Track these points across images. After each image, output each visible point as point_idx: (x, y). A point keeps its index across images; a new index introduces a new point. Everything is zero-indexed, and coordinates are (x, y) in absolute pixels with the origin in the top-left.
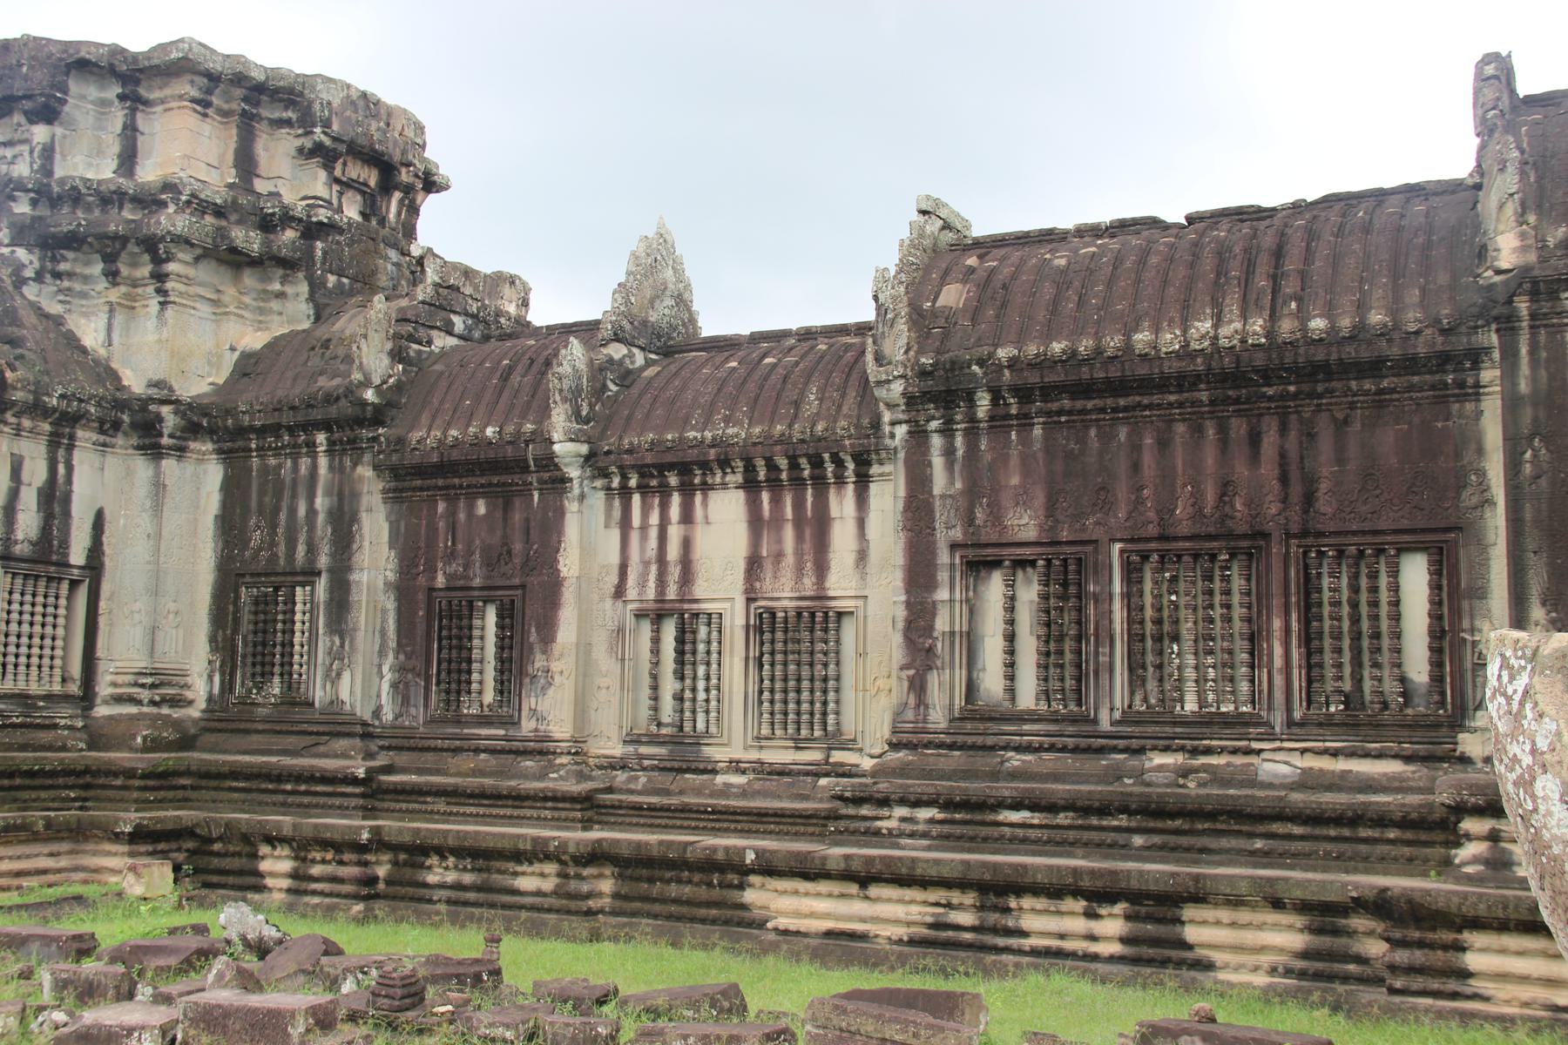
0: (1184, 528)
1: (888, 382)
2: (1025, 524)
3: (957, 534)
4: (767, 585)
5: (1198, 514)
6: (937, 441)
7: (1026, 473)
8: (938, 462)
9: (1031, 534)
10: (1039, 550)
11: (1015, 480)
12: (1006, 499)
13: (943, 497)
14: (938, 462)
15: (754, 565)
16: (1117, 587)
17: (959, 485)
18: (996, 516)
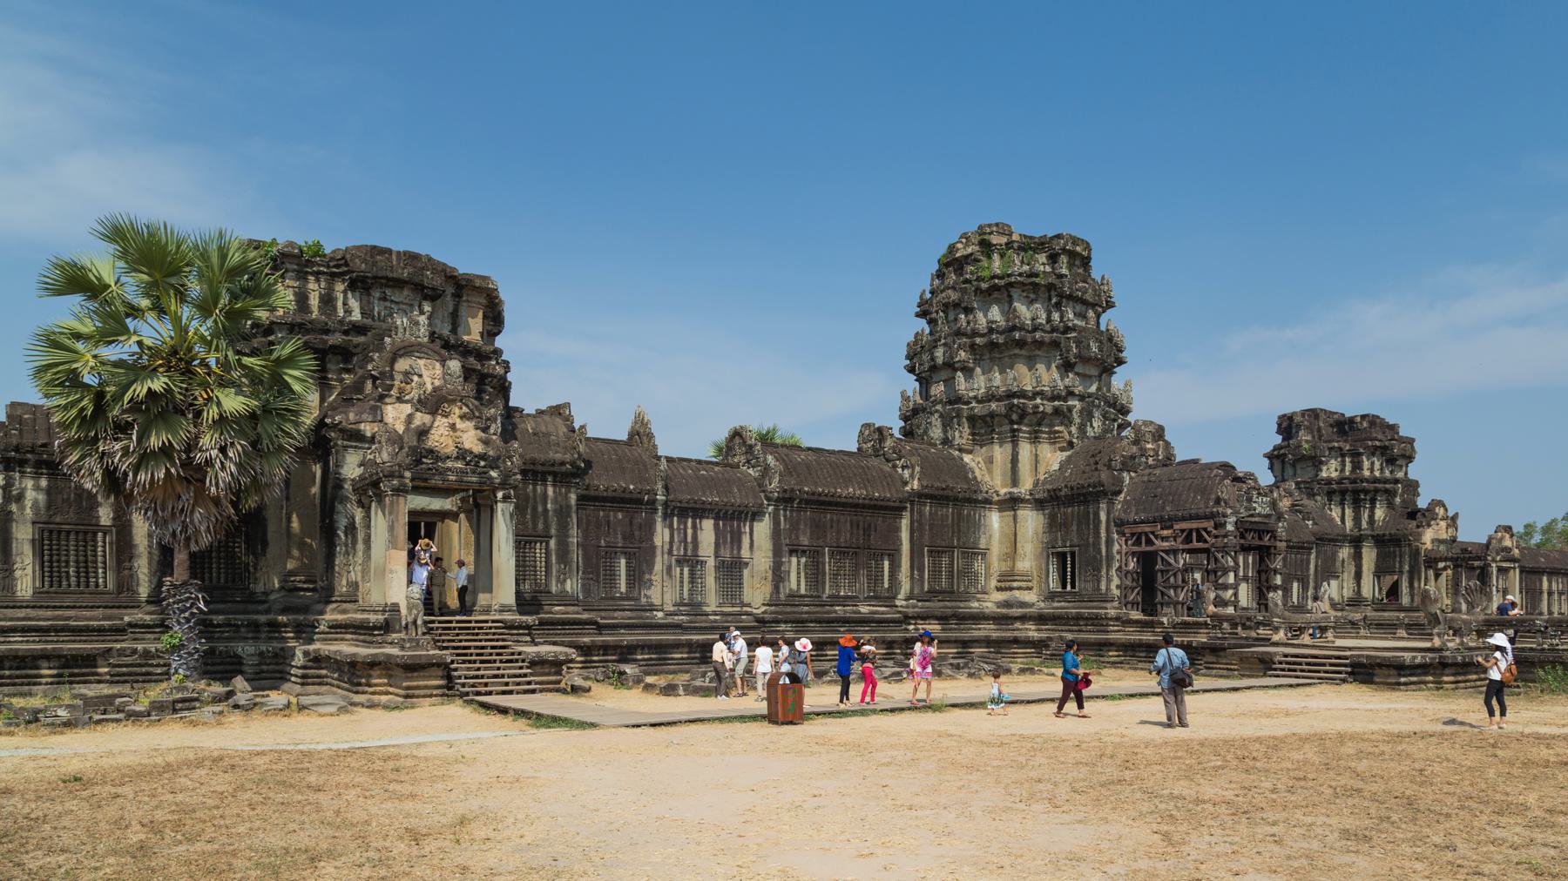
2: (805, 540)
4: (722, 552)
15: (717, 545)
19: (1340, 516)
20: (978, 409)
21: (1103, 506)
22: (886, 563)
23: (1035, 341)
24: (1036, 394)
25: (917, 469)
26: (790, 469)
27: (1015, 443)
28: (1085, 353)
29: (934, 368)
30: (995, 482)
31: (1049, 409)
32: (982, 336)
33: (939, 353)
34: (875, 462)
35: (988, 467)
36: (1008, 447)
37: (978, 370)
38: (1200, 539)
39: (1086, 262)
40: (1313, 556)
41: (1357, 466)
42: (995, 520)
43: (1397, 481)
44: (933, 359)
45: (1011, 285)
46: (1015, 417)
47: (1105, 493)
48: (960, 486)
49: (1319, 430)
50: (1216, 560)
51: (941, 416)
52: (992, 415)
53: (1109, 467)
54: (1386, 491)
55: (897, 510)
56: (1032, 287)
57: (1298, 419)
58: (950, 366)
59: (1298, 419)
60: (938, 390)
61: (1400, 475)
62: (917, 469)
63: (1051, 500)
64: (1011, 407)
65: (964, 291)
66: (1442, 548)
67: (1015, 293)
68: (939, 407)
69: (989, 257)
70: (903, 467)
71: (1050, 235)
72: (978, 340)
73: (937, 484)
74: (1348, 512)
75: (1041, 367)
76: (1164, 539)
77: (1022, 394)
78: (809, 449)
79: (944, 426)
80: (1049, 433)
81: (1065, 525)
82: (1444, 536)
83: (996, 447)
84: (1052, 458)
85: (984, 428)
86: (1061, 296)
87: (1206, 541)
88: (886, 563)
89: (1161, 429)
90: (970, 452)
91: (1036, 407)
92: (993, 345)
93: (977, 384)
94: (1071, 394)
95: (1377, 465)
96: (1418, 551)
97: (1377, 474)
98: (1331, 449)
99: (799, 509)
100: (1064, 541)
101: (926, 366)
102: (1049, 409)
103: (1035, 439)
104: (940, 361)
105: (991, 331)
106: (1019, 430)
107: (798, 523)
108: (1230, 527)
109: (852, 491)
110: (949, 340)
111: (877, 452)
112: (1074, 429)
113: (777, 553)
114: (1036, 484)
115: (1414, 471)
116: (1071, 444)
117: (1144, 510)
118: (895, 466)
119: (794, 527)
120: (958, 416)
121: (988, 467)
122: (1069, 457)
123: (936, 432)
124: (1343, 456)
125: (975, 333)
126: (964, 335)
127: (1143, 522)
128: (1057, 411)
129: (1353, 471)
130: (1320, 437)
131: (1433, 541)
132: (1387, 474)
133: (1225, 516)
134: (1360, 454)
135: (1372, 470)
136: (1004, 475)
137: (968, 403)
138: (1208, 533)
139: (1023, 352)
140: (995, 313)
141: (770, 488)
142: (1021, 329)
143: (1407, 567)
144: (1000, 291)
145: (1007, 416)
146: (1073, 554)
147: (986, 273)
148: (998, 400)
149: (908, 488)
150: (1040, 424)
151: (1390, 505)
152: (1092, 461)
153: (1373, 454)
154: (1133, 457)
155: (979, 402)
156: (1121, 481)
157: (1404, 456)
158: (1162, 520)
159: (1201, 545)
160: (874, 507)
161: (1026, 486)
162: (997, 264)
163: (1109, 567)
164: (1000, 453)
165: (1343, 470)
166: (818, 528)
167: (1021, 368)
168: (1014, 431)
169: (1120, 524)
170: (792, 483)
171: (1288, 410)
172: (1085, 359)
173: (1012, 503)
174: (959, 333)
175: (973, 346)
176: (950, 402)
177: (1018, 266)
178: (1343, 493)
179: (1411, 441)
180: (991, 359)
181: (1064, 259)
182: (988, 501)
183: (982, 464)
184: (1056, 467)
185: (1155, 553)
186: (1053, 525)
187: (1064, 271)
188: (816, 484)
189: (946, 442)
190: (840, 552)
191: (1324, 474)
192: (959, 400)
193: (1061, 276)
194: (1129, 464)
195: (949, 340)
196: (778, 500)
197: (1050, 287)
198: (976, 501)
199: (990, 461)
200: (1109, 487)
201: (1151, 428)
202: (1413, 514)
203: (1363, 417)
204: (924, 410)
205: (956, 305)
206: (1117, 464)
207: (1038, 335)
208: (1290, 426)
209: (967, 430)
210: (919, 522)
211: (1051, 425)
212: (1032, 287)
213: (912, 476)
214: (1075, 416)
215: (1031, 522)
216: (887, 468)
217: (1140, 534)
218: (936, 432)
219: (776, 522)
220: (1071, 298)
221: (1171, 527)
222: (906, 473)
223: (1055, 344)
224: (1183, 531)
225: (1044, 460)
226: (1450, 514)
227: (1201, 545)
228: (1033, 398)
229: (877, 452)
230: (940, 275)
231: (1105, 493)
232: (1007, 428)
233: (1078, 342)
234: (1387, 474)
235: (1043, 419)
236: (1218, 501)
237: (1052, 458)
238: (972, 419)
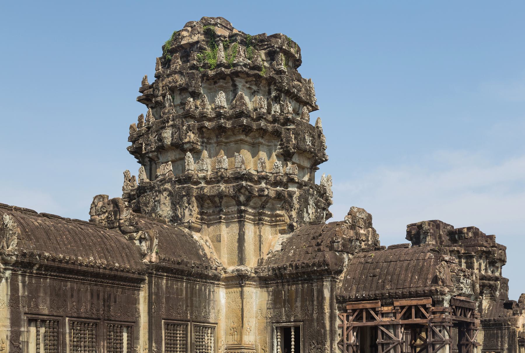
0: (83, 315)
1: (12, 255)
2: (44, 309)
3: (26, 310)
5: (86, 312)
6: (20, 278)
7: (46, 293)
8: (20, 284)
9: (46, 312)
10: (48, 317)
11: (41, 294)
12: (40, 300)
13: (22, 296)
14: (20, 284)
16: (68, 331)
17: (26, 293)
18: (37, 306)
20: (208, 190)
21: (327, 284)
22: (125, 335)
23: (260, 129)
24: (262, 178)
25: (156, 241)
26: (28, 233)
27: (241, 223)
28: (301, 145)
29: (161, 149)
30: (223, 260)
31: (272, 194)
32: (210, 120)
33: (168, 135)
34: (111, 233)
35: (217, 245)
36: (235, 227)
37: (205, 153)
38: (419, 314)
39: (297, 63)
42: (222, 297)
43: (497, 279)
44: (161, 139)
45: (236, 74)
46: (242, 198)
47: (328, 272)
48: (194, 262)
49: (440, 237)
50: (434, 333)
51: (170, 194)
52: (221, 195)
53: (331, 248)
54: (490, 286)
55: (135, 282)
56: (255, 79)
57: (426, 227)
58: (179, 147)
59: (426, 227)
60: (165, 169)
61: (497, 274)
62: (156, 241)
63: (276, 279)
64: (239, 189)
65: (191, 77)
67: (240, 83)
68: (168, 186)
69: (213, 47)
70: (141, 240)
71: (268, 34)
72: (207, 124)
73: (173, 258)
75: (263, 155)
76: (383, 315)
77: (248, 177)
78: (44, 215)
79: (174, 205)
80: (271, 216)
81: (289, 302)
83: (223, 227)
84: (274, 241)
85: (212, 208)
86: (280, 90)
87: (424, 317)
88: (125, 335)
89: (370, 217)
90: (199, 230)
91: (262, 190)
92: (221, 130)
93: (202, 166)
94: (291, 181)
95: (483, 267)
96: (514, 332)
97: (483, 272)
99: (39, 276)
100: (288, 316)
101: (154, 146)
102: (272, 194)
103: (258, 221)
104: (168, 141)
105: (219, 115)
106: (245, 211)
107: (37, 290)
108: (446, 305)
109: (92, 259)
110: (178, 122)
111: (111, 224)
112: (294, 213)
113: (15, 322)
114: (260, 263)
115: (506, 272)
116: (291, 228)
117: (365, 289)
118: (132, 239)
119: (33, 294)
120: (188, 195)
121: (217, 245)
122: (290, 241)
123: (165, 210)
124: (460, 257)
125: (203, 117)
126: (193, 117)
127: (364, 299)
128: (279, 196)
130: (441, 242)
132: (490, 273)
133: (443, 294)
134: (472, 257)
136: (230, 253)
137: (197, 183)
138: (426, 309)
139: (248, 139)
140: (222, 99)
141: (7, 250)
142: (248, 116)
143: (506, 346)
144: (225, 78)
145: (235, 197)
146: (297, 329)
147: (211, 61)
148: (226, 182)
149: (146, 260)
150: (263, 207)
151: (493, 297)
152: (314, 242)
153: (481, 257)
154: (350, 241)
155: (208, 183)
156: (342, 261)
158: (382, 297)
159: (419, 321)
160: (114, 278)
161: (250, 265)
162: (222, 55)
163: (332, 340)
164: (227, 232)
166: (58, 297)
167: (245, 154)
168: (240, 212)
169: (342, 301)
170: (30, 247)
171: (417, 220)
172: (301, 151)
173: (239, 280)
174: (188, 115)
175: (201, 130)
176: (179, 181)
177: (242, 58)
179: (504, 249)
180: (218, 143)
181: (281, 57)
182: (216, 278)
183: (209, 243)
184: (279, 248)
185: (375, 329)
186: (277, 301)
187: (283, 67)
188: (55, 250)
189: (175, 219)
190: (79, 322)
192: (188, 179)
193: (280, 72)
194: (347, 247)
195: (178, 122)
196: (16, 264)
197: (271, 81)
198: (207, 277)
199: (218, 239)
200: (333, 267)
201: (363, 216)
202: (509, 305)
203: (469, 229)
204: (152, 188)
205: (183, 90)
206: (338, 245)
207: (263, 123)
208: (418, 234)
209: (196, 209)
210: (157, 294)
211: (273, 209)
212: (255, 79)
213: (150, 248)
214: (295, 201)
215: (256, 298)
216: (124, 239)
217: (361, 310)
218: (165, 210)
219: (14, 289)
220: (288, 93)
221: (392, 304)
222: (144, 246)
223: (277, 134)
224: (402, 307)
225: (267, 242)
227: (419, 321)
228: (259, 182)
229: (111, 224)
230: (165, 62)
231: (328, 272)
232: (235, 209)
233: (297, 134)
234: (490, 273)
235: (266, 202)
236: (435, 280)
237: (274, 241)
238: (201, 199)
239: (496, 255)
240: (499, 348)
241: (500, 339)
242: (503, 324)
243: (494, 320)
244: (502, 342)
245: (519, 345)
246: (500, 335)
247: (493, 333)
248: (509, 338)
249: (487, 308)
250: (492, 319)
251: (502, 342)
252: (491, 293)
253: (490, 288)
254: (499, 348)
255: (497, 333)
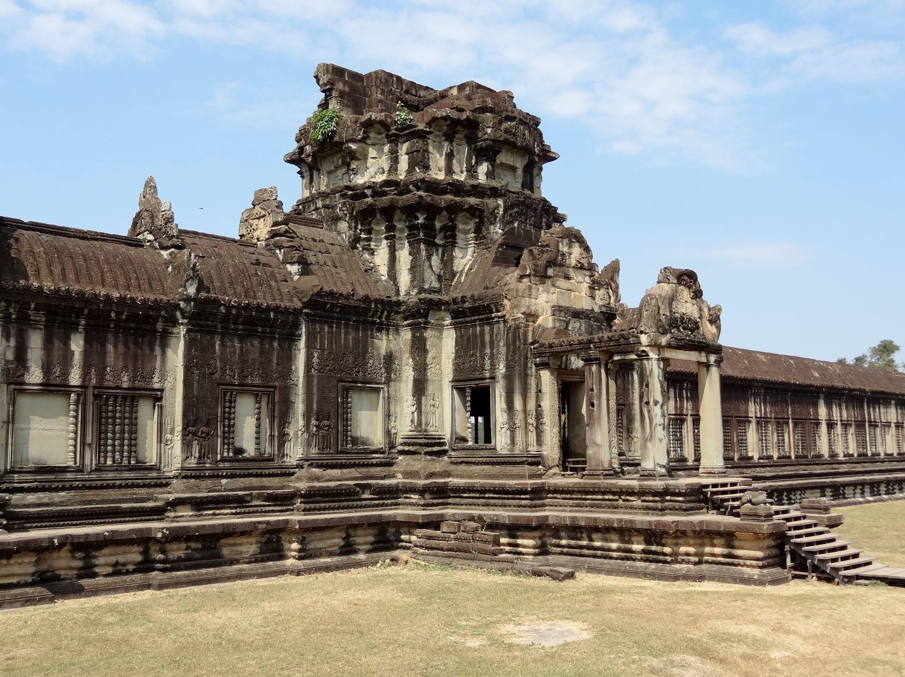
19: (391, 266)
40: (302, 343)
41: (419, 160)
54: (474, 212)
66: (574, 325)
74: (404, 256)
82: (585, 304)
98: (368, 125)
129: (410, 170)
131: (558, 310)
132: (482, 178)
135: (449, 171)
143: (502, 369)
157: (512, 147)
165: (393, 168)
178: (388, 213)
191: (360, 180)
226: (601, 261)
239: (489, 131)
240: (488, 375)
241: (488, 351)
242: (493, 306)
243: (473, 296)
244: (492, 357)
245: (537, 365)
246: (487, 338)
247: (474, 334)
248: (508, 345)
249: (466, 269)
250: (469, 295)
251: (492, 357)
252: (478, 230)
253: (473, 215)
254: (488, 375)
255: (482, 333)
